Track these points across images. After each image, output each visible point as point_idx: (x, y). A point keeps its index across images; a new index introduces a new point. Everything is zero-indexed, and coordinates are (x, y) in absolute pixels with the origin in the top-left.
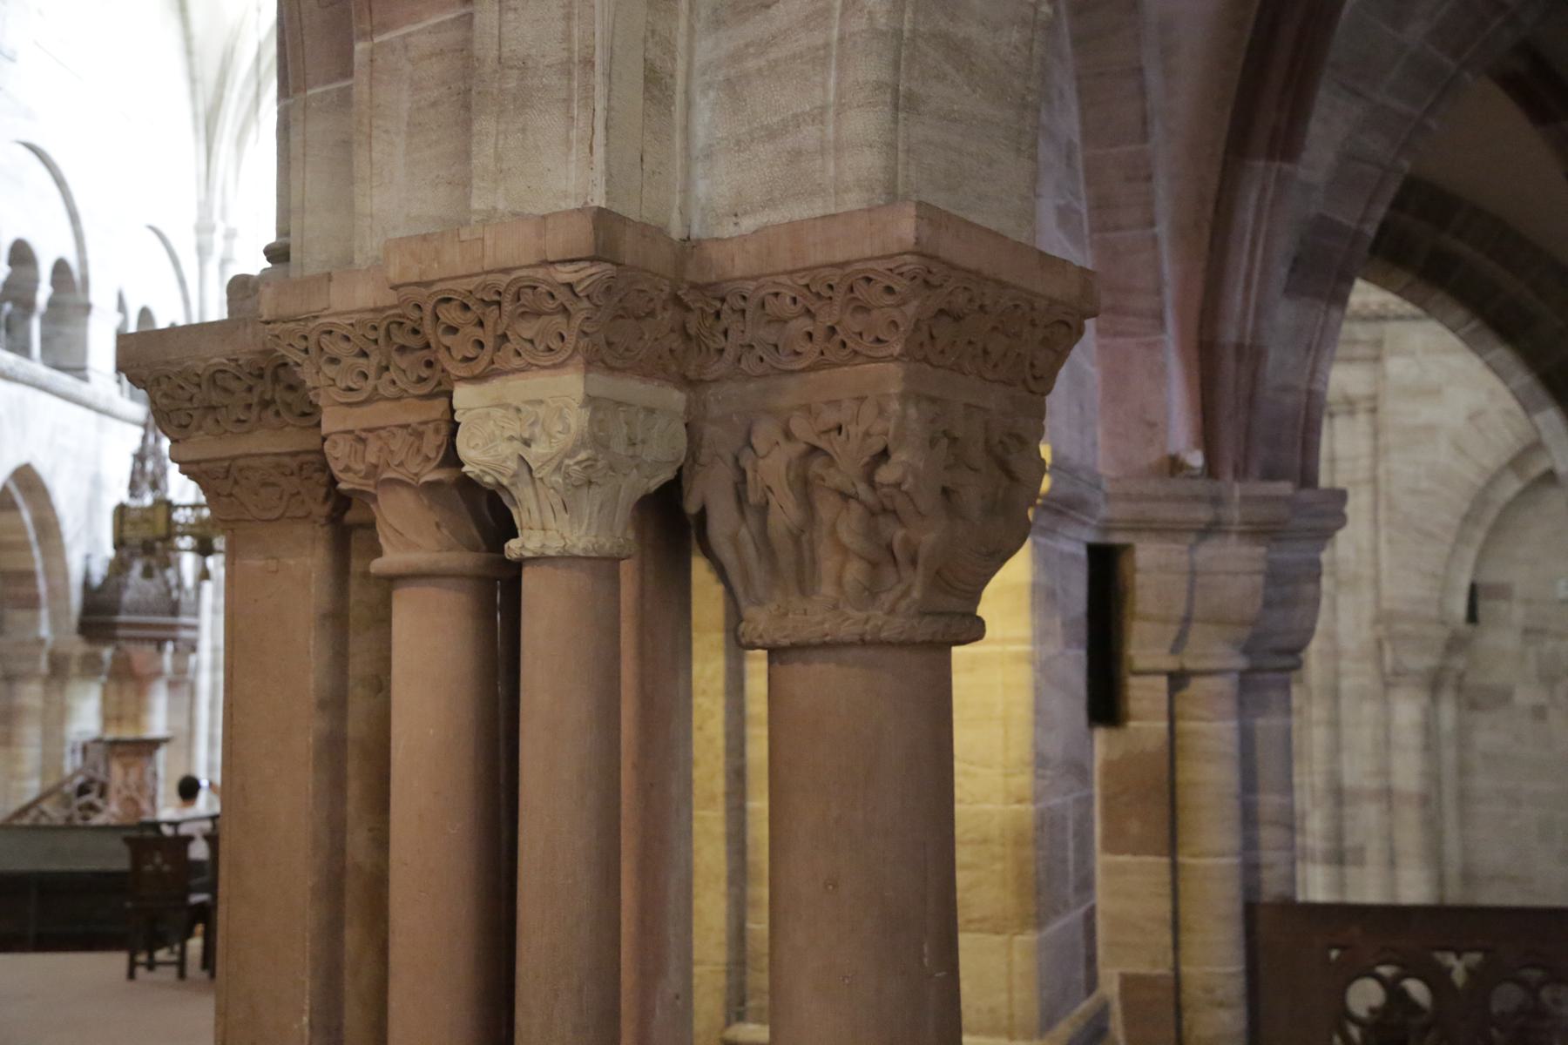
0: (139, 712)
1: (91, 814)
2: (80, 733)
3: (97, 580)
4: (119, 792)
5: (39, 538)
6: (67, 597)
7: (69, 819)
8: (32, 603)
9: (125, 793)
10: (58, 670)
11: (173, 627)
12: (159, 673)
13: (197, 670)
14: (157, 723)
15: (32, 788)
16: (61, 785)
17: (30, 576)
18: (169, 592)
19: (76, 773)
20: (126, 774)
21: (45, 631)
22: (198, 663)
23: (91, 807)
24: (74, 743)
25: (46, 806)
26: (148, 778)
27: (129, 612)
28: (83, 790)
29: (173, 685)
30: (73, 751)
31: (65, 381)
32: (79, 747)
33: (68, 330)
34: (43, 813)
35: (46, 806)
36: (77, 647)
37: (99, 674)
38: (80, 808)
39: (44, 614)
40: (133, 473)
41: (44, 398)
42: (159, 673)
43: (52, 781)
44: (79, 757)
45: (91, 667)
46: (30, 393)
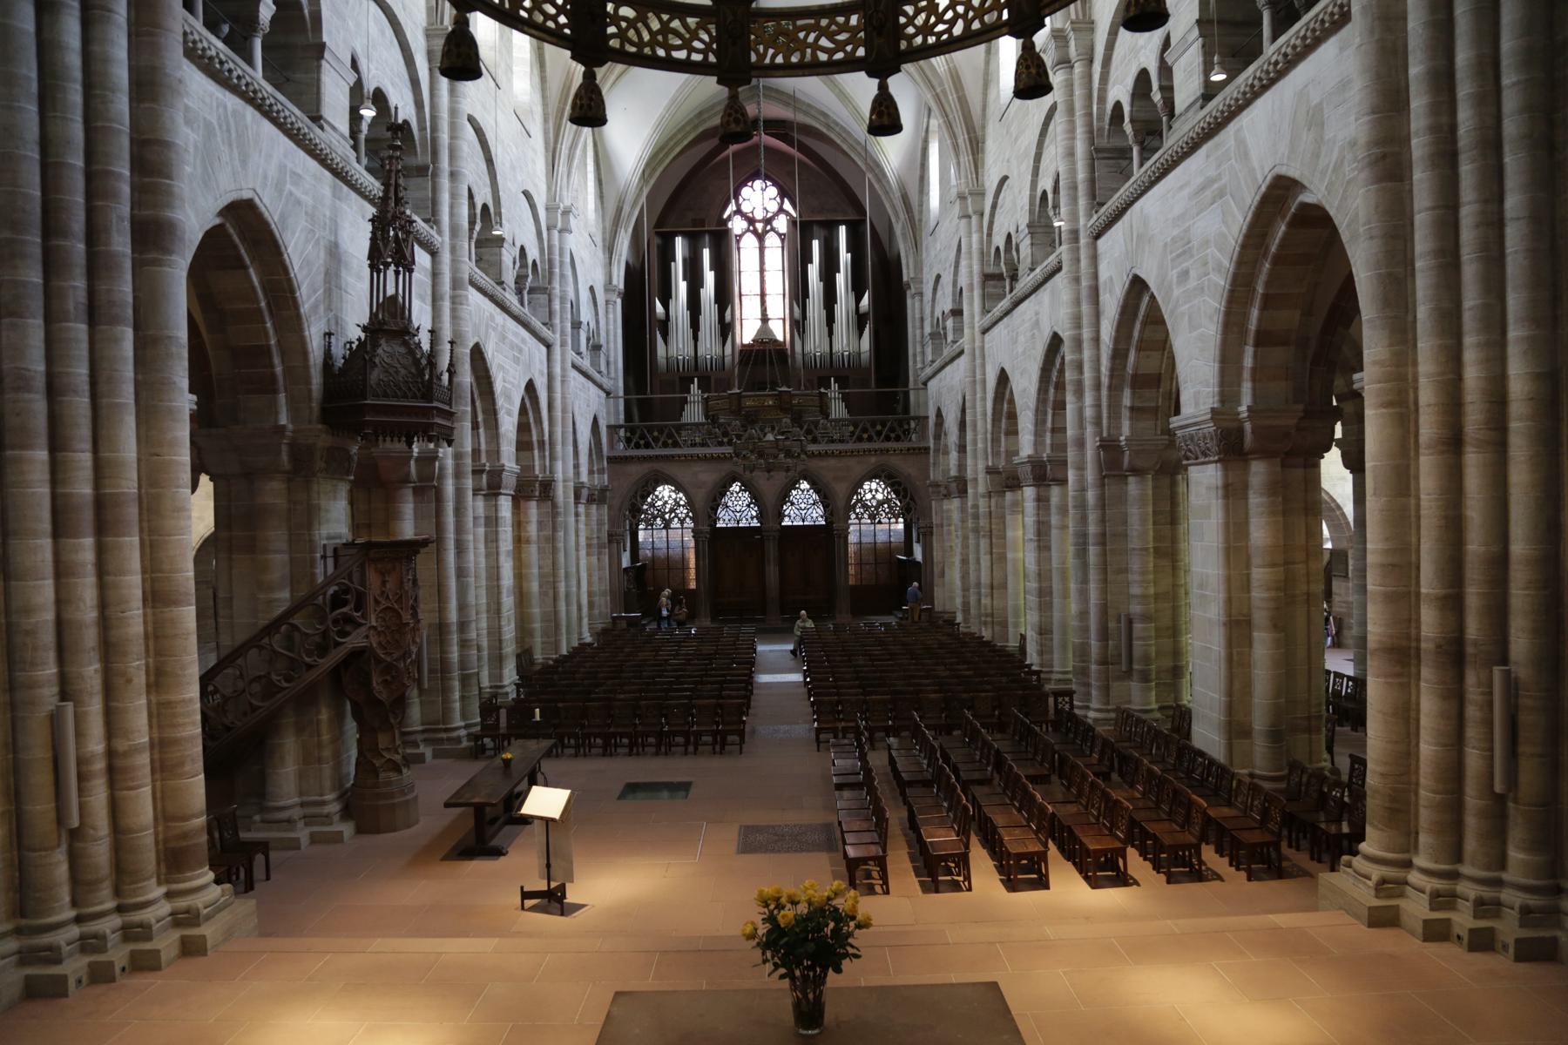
0: (391, 516)
1: (348, 628)
2: (329, 538)
3: (340, 363)
4: (377, 602)
5: (268, 304)
6: (307, 380)
7: (325, 634)
8: (268, 386)
9: (384, 604)
10: (303, 469)
11: (427, 412)
12: (406, 480)
13: (441, 477)
14: (407, 529)
15: (285, 595)
16: (313, 595)
17: (266, 351)
18: (421, 373)
19: (329, 581)
20: (384, 583)
21: (283, 420)
22: (442, 469)
23: (348, 619)
24: (325, 546)
25: (297, 620)
26: (408, 586)
27: (376, 396)
28: (337, 601)
29: (418, 492)
30: (324, 557)
31: (294, 113)
32: (330, 553)
33: (298, 76)
34: (295, 628)
35: (297, 620)
36: (323, 440)
37: (348, 473)
38: (335, 622)
39: (282, 397)
40: (373, 240)
41: (267, 126)
42: (406, 480)
43: (303, 591)
44: (330, 562)
45: (337, 464)
46: (250, 113)
